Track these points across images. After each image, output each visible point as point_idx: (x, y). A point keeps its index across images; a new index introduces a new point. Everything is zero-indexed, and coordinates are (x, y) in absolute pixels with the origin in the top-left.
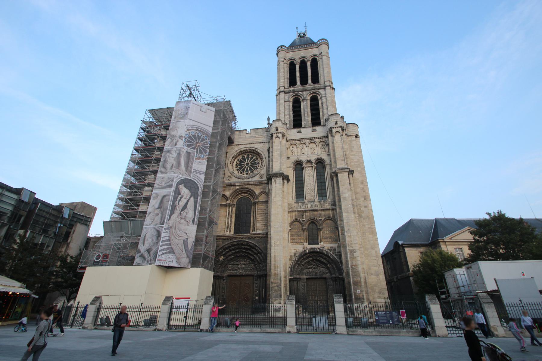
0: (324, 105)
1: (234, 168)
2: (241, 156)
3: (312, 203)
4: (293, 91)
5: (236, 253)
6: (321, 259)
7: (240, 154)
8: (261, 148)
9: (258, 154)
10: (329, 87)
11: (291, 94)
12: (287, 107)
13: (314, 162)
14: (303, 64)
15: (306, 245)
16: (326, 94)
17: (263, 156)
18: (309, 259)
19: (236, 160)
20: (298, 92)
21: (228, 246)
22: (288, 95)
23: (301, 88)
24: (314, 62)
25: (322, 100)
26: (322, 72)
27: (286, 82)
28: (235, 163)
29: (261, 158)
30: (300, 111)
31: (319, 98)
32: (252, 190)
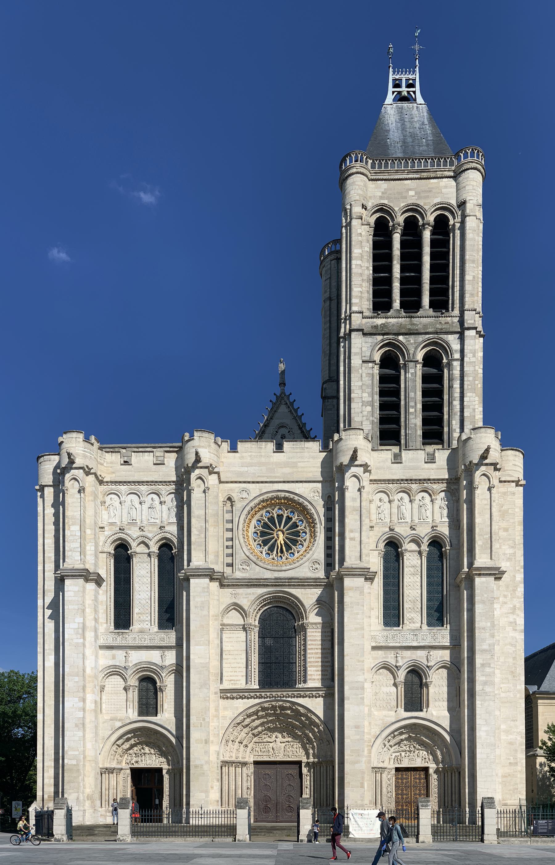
0: (457, 385)
1: (251, 539)
3: (417, 632)
5: (268, 722)
7: (264, 507)
11: (380, 338)
12: (367, 380)
14: (412, 227)
15: (401, 710)
16: (462, 351)
17: (316, 516)
19: (254, 521)
22: (369, 339)
24: (442, 226)
27: (366, 295)
29: (312, 524)
31: (445, 361)
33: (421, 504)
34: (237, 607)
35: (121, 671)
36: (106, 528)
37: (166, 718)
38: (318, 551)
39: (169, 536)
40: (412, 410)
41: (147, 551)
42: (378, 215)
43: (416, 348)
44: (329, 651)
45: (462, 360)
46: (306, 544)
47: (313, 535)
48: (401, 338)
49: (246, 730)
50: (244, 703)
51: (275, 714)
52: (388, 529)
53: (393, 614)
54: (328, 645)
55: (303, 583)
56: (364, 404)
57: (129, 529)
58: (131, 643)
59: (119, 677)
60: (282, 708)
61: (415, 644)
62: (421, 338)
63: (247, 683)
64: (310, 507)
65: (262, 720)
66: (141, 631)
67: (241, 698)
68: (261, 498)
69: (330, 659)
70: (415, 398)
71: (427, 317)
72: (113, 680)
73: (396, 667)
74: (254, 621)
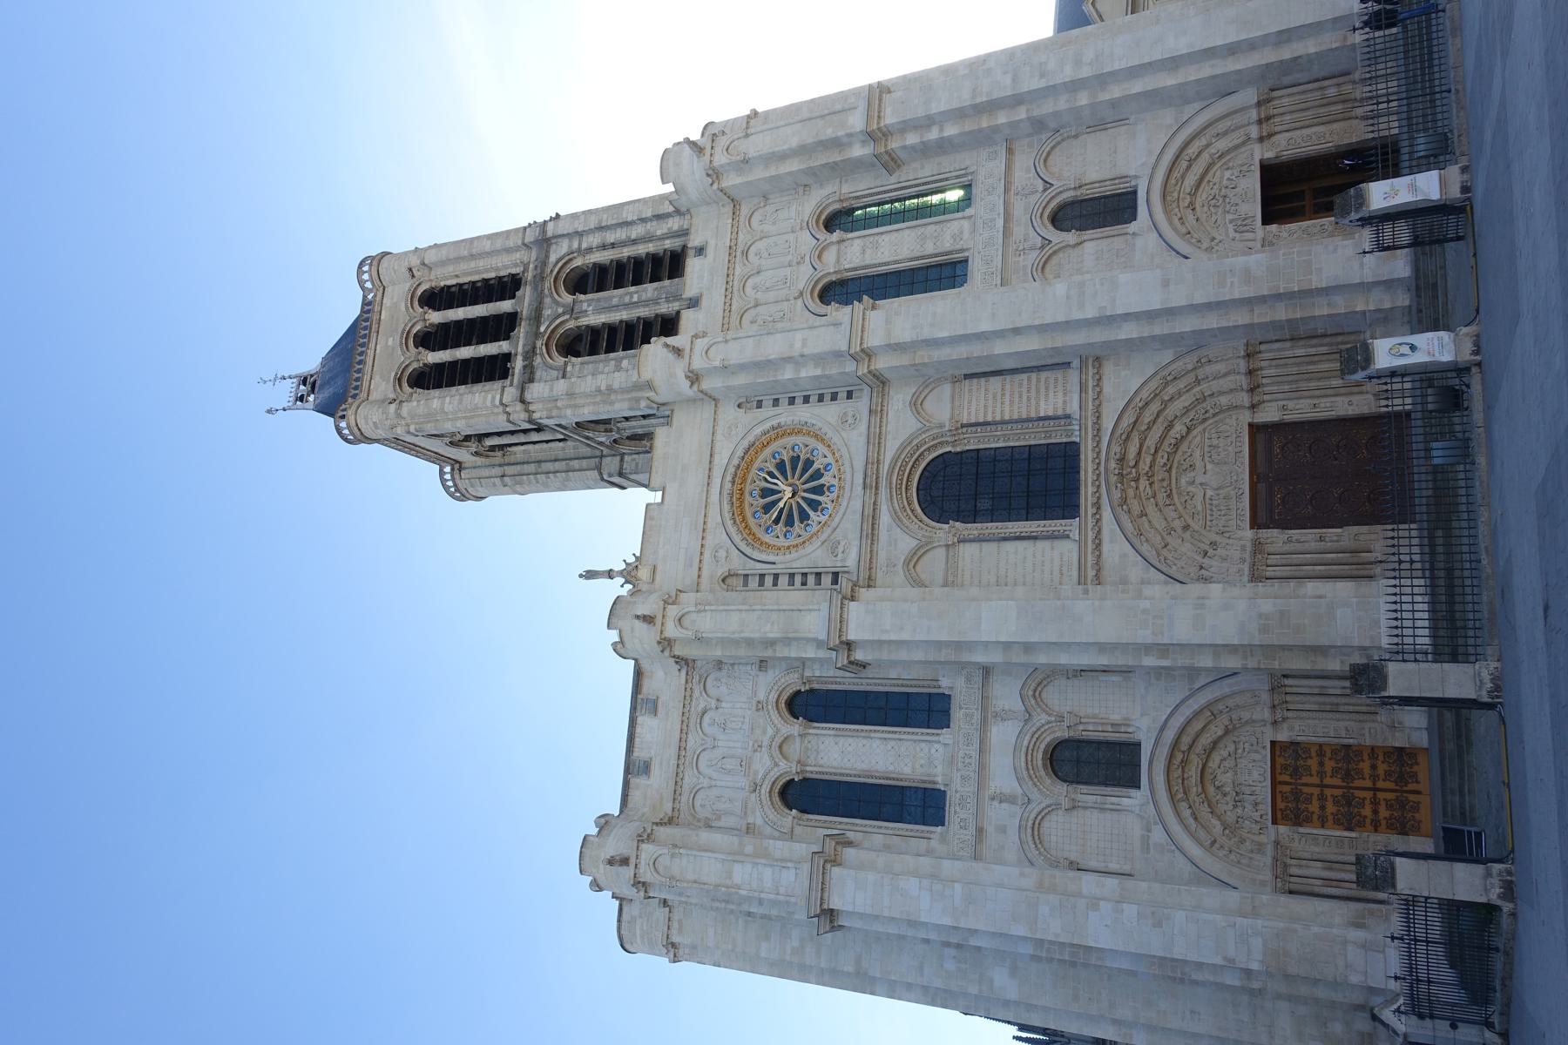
0: (611, 237)
2: (751, 521)
4: (530, 354)
6: (1191, 179)
8: (736, 430)
9: (752, 451)
10: (550, 226)
11: (538, 360)
13: (823, 235)
15: (1133, 227)
16: (569, 236)
17: (767, 426)
18: (1190, 218)
19: (767, 538)
20: (537, 335)
21: (1125, 519)
22: (538, 374)
23: (522, 332)
24: (435, 298)
25: (590, 250)
26: (481, 264)
28: (782, 542)
29: (779, 432)
30: (612, 329)
31: (578, 262)
32: (902, 448)
33: (765, 255)
34: (914, 559)
35: (1033, 816)
36: (751, 820)
37: (1142, 716)
38: (823, 416)
39: (773, 696)
40: (635, 298)
41: (798, 740)
42: (405, 385)
43: (558, 304)
44: (1008, 378)
45: (580, 234)
46: (813, 443)
47: (797, 431)
48: (542, 329)
49: (1174, 542)
50: (1111, 542)
51: (1137, 480)
52: (799, 302)
53: (945, 274)
54: (995, 382)
55: (875, 440)
56: (618, 368)
57: (756, 773)
58: (971, 788)
59: (1046, 824)
60: (1122, 460)
61: (1000, 222)
62: (547, 300)
63: (1068, 537)
64: (751, 438)
65: (1151, 509)
66: (951, 761)
67: (1098, 546)
68: (729, 523)
69: (1024, 376)
70: (621, 297)
71: (523, 302)
72: (1053, 838)
73: (1042, 247)
74: (944, 532)
